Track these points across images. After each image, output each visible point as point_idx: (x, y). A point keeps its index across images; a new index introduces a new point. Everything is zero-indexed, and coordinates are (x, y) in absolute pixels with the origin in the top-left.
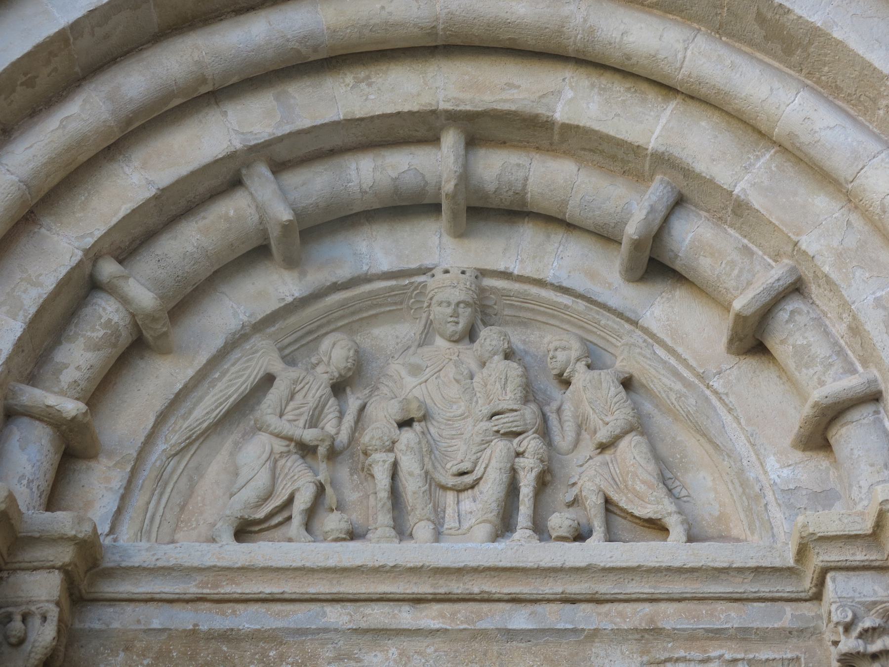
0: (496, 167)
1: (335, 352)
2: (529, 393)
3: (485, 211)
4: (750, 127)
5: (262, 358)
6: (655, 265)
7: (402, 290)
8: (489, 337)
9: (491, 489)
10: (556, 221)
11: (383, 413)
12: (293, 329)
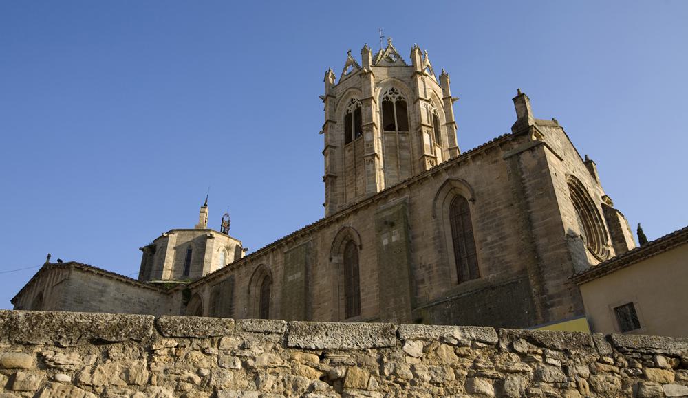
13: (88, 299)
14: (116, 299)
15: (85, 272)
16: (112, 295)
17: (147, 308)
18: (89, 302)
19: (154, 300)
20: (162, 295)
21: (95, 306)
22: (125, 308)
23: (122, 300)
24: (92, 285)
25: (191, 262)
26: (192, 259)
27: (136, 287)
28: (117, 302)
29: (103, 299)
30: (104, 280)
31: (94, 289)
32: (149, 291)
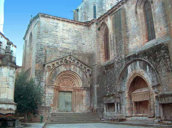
14: (63, 30)
15: (46, 17)
16: (61, 28)
17: (79, 33)
19: (82, 29)
20: (85, 27)
21: (54, 34)
22: (69, 34)
23: (66, 30)
24: (51, 24)
25: (96, 12)
26: (97, 10)
27: (72, 24)
28: (64, 31)
29: (57, 30)
30: (56, 21)
32: (79, 25)
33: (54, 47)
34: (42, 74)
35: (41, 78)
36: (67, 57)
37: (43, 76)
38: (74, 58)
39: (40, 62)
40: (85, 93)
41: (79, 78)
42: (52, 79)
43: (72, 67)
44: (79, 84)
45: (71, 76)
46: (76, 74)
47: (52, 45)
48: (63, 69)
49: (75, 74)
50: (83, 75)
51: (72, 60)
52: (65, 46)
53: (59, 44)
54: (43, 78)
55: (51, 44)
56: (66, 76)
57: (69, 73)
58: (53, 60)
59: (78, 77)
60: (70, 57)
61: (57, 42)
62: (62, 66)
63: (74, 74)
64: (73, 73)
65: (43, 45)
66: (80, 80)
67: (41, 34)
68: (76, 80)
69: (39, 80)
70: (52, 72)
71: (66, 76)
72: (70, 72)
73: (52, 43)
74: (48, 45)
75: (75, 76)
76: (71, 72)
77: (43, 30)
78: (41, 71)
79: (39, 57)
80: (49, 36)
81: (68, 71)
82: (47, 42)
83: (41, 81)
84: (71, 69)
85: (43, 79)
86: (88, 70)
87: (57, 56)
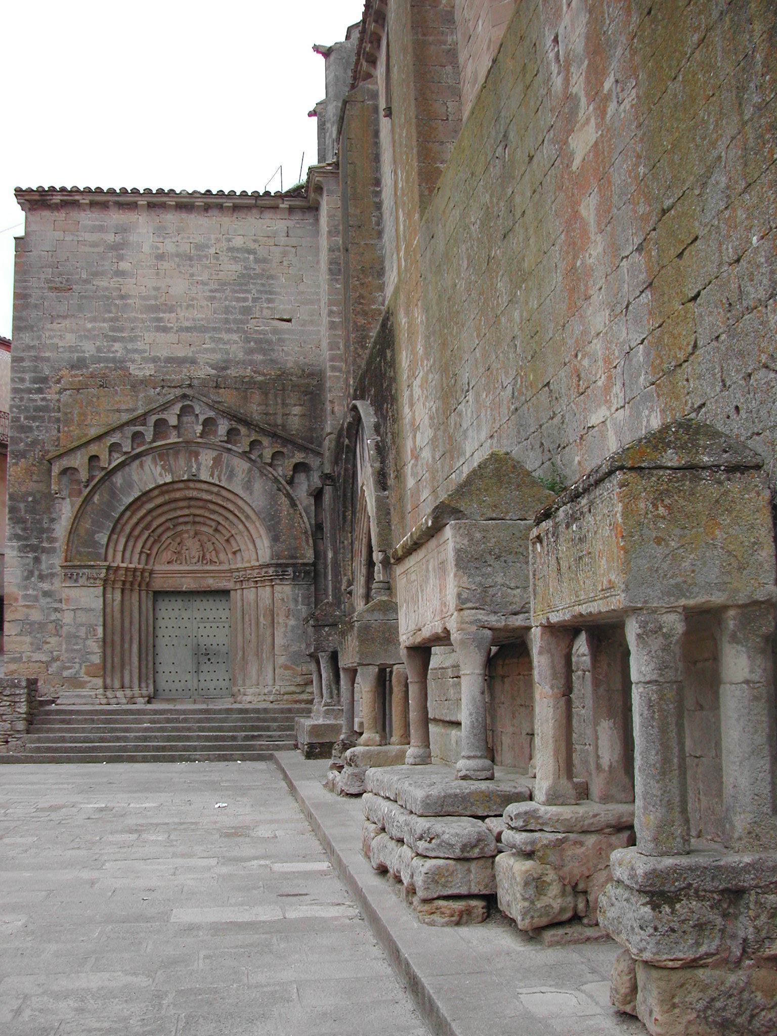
0: (198, 519)
1: (178, 540)
2: (201, 545)
3: (194, 523)
4: (227, 519)
5: (169, 541)
6: (216, 530)
7: (187, 532)
8: (196, 539)
9: (197, 558)
10: (204, 524)
11: (185, 548)
12: (173, 537)
13: (84, 276)
18: (86, 281)
31: (94, 245)
33: (107, 360)
34: (48, 510)
35: (44, 532)
36: (165, 407)
37: (52, 520)
38: (212, 408)
39: (38, 453)
40: (285, 590)
41: (250, 512)
42: (94, 532)
43: (207, 458)
44: (258, 549)
45: (211, 506)
46: (231, 496)
47: (99, 350)
48: (150, 474)
49: (224, 493)
50: (273, 498)
51: (202, 418)
52: (165, 345)
53: (133, 339)
54: (50, 530)
55: (89, 349)
56: (186, 512)
57: (195, 494)
58: (93, 432)
59: (246, 508)
60: (183, 409)
61: (121, 330)
62: (148, 461)
63: (217, 494)
64: (215, 489)
65: (47, 360)
66: (258, 525)
67: (32, 301)
68: (241, 527)
69: (35, 541)
70: (87, 500)
71: (186, 512)
72: (198, 485)
73: (98, 343)
74: (75, 356)
75: (230, 506)
76: (205, 486)
77: (48, 281)
78: (38, 496)
79: (31, 428)
80: (80, 308)
81: (181, 485)
82: (70, 339)
83: (44, 550)
84: (198, 469)
85: (52, 540)
86: (300, 467)
87: (119, 411)
